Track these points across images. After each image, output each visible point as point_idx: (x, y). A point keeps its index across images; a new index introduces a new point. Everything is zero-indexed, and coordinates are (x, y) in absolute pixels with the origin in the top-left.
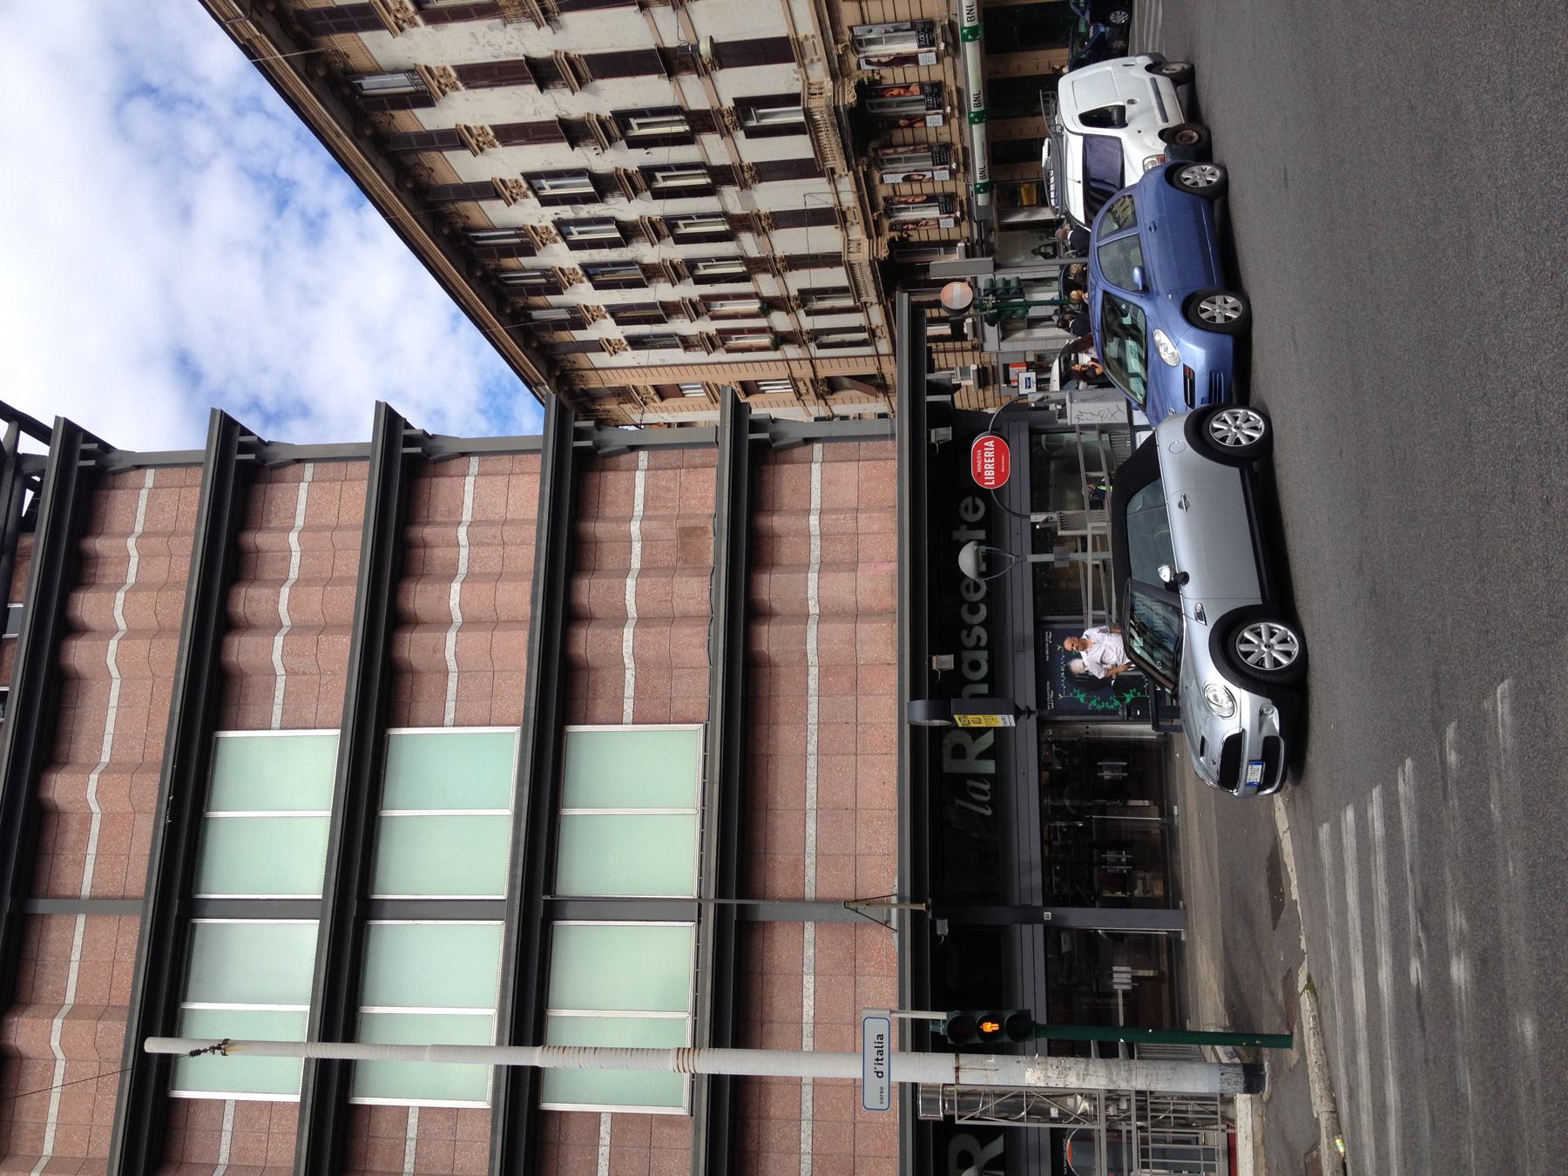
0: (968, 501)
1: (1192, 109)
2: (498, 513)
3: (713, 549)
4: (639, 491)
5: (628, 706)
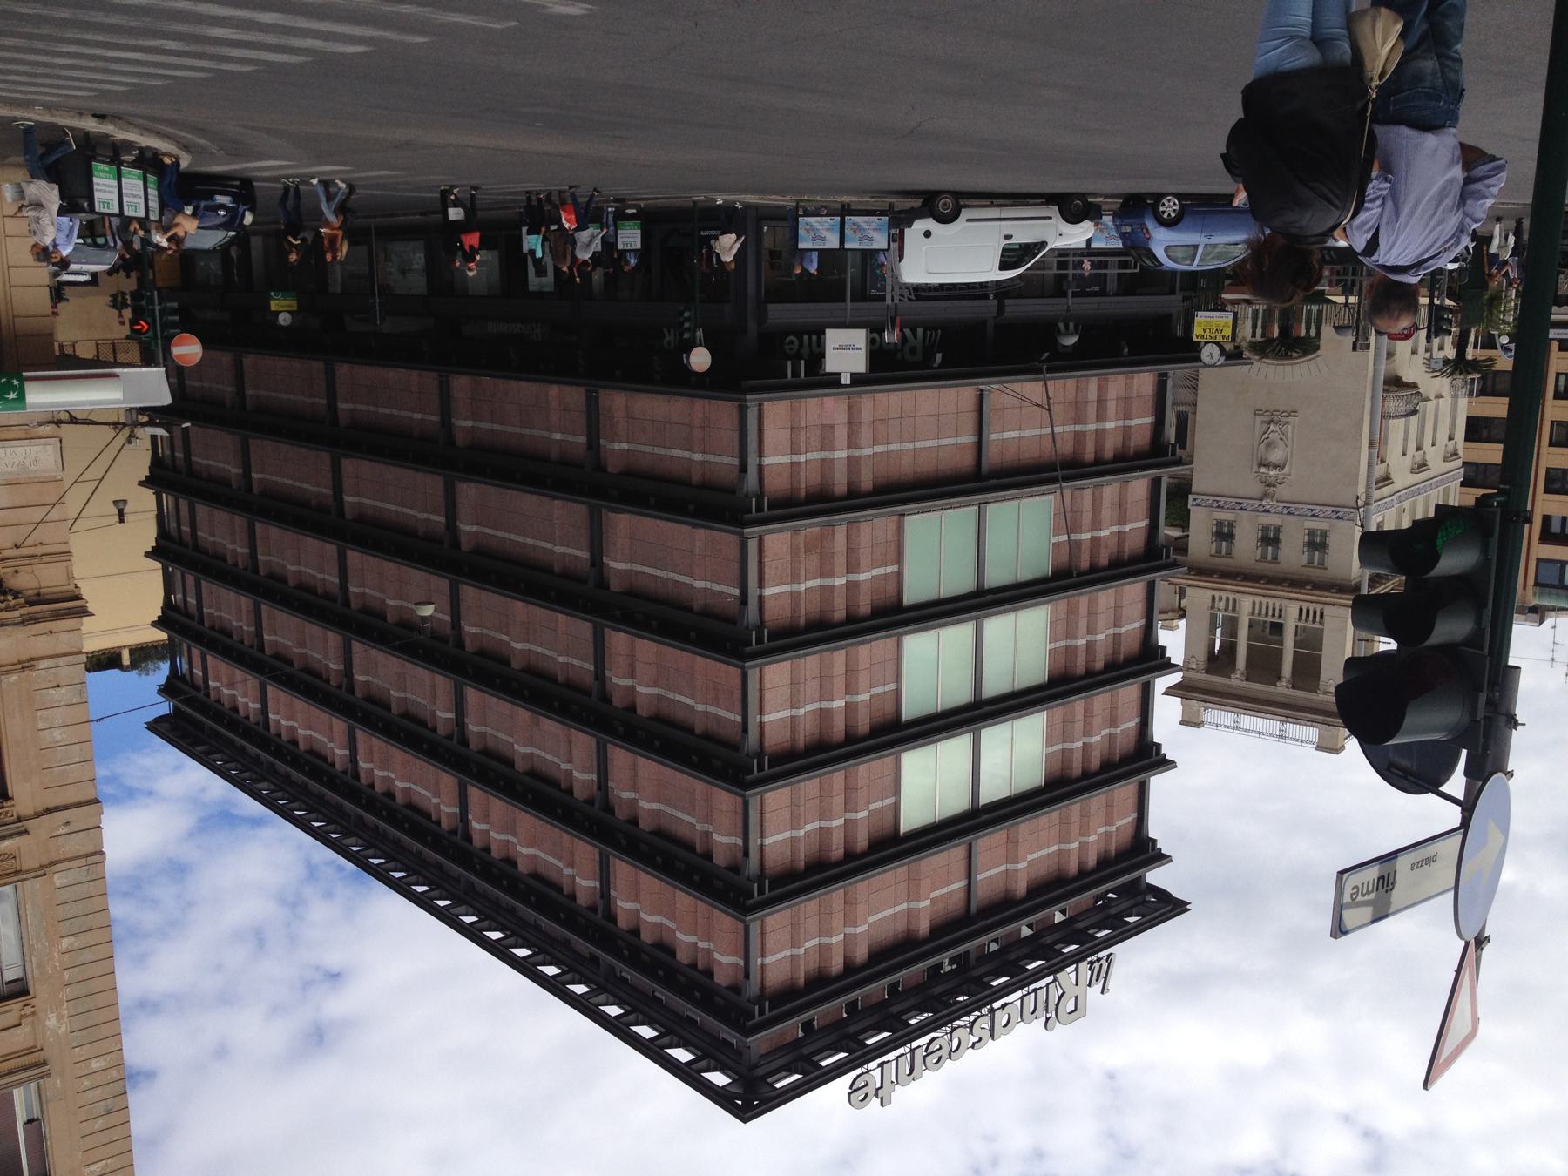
1: (1050, 199)
2: (786, 691)
3: (810, 528)
4: (777, 590)
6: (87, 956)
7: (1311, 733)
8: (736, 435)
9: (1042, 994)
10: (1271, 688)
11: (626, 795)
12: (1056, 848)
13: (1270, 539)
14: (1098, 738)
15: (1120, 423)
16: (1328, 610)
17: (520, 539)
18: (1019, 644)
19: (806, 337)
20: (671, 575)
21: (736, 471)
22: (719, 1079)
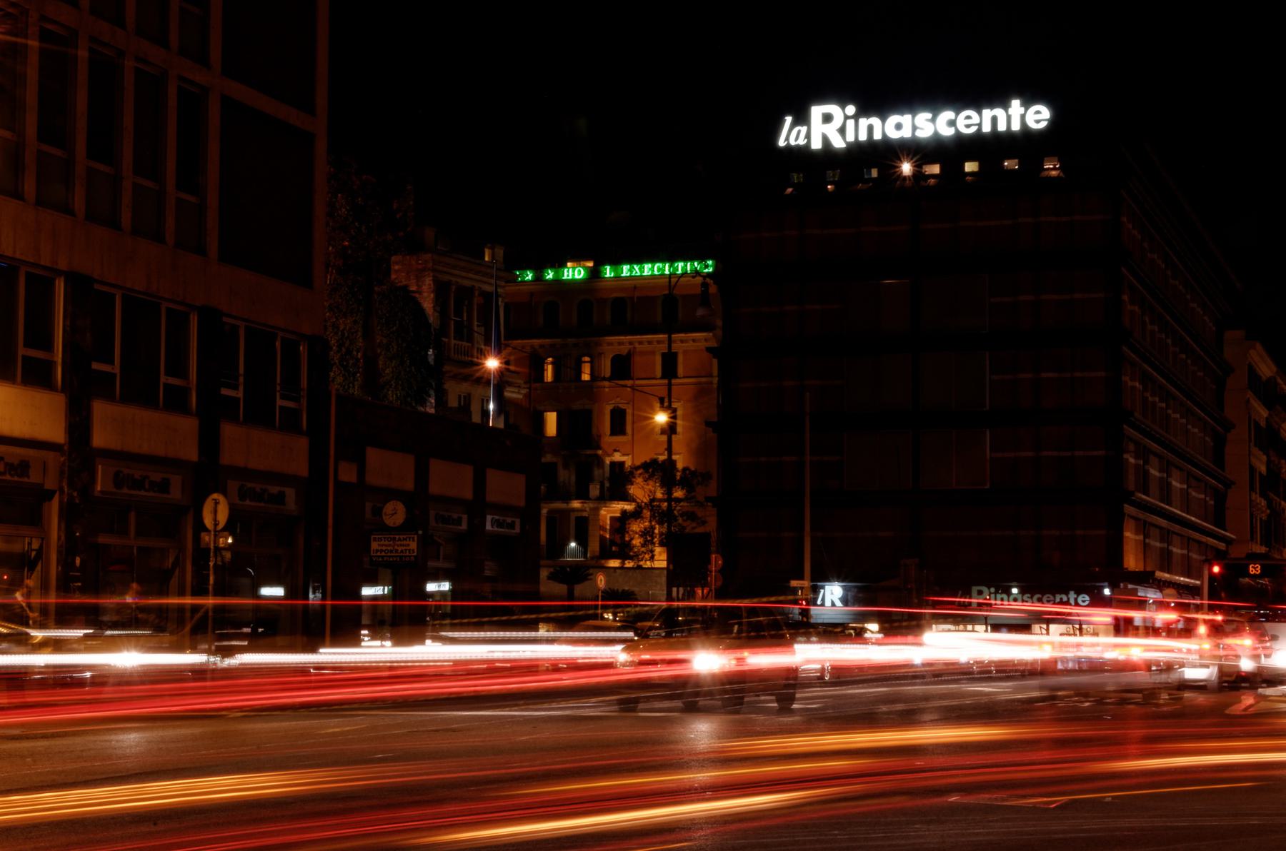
0: (1087, 598)
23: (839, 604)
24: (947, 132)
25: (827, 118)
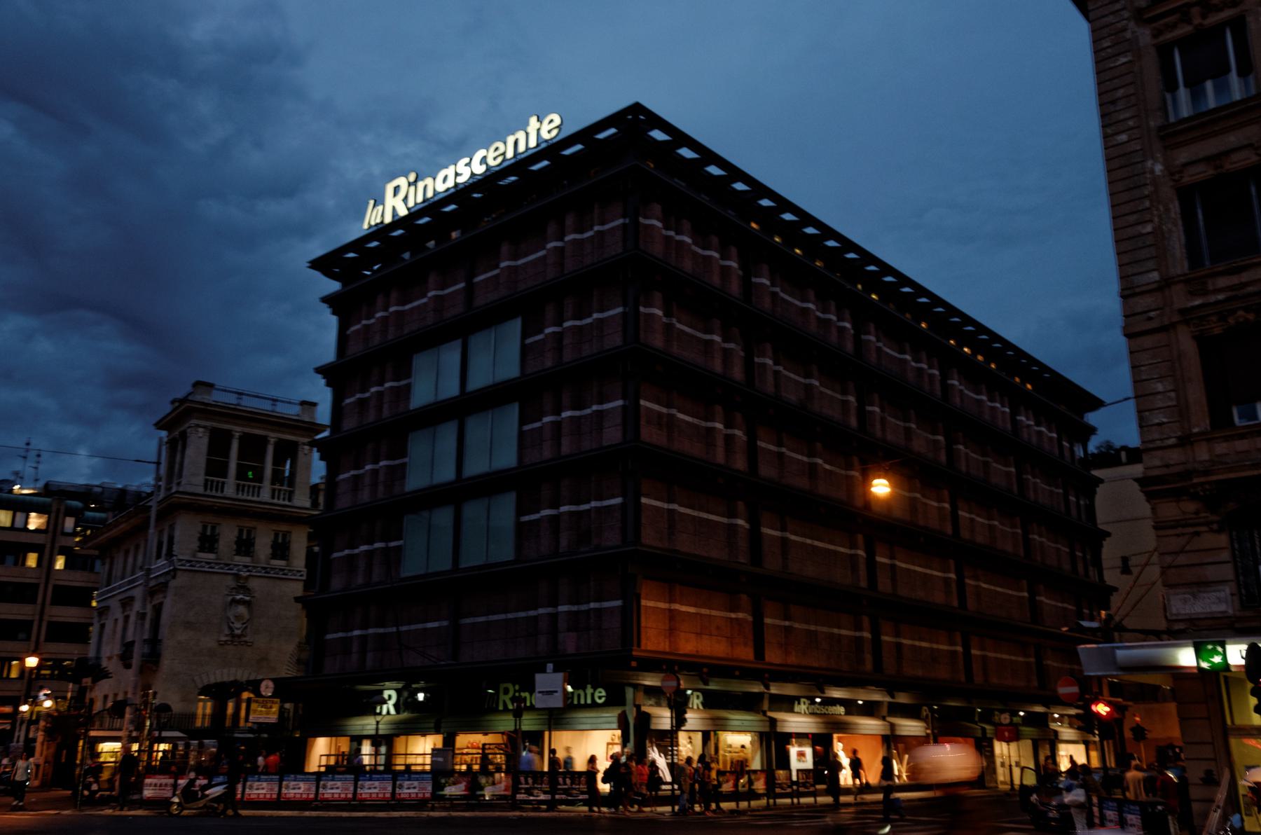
0: (604, 694)
5: (526, 518)
6: (1132, 219)
7: (216, 397)
8: (643, 624)
9: (420, 199)
10: (247, 430)
11: (732, 346)
12: (407, 307)
13: (245, 546)
14: (373, 390)
15: (349, 634)
16: (200, 490)
17: (816, 543)
18: (431, 462)
19: (589, 701)
20: (695, 513)
21: (643, 595)
22: (658, 135)
23: (393, 711)
24: (480, 169)
25: (396, 190)
